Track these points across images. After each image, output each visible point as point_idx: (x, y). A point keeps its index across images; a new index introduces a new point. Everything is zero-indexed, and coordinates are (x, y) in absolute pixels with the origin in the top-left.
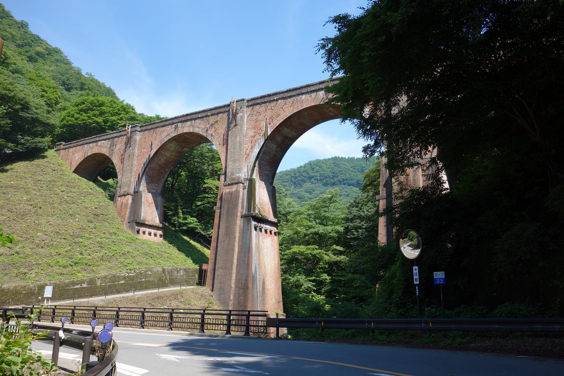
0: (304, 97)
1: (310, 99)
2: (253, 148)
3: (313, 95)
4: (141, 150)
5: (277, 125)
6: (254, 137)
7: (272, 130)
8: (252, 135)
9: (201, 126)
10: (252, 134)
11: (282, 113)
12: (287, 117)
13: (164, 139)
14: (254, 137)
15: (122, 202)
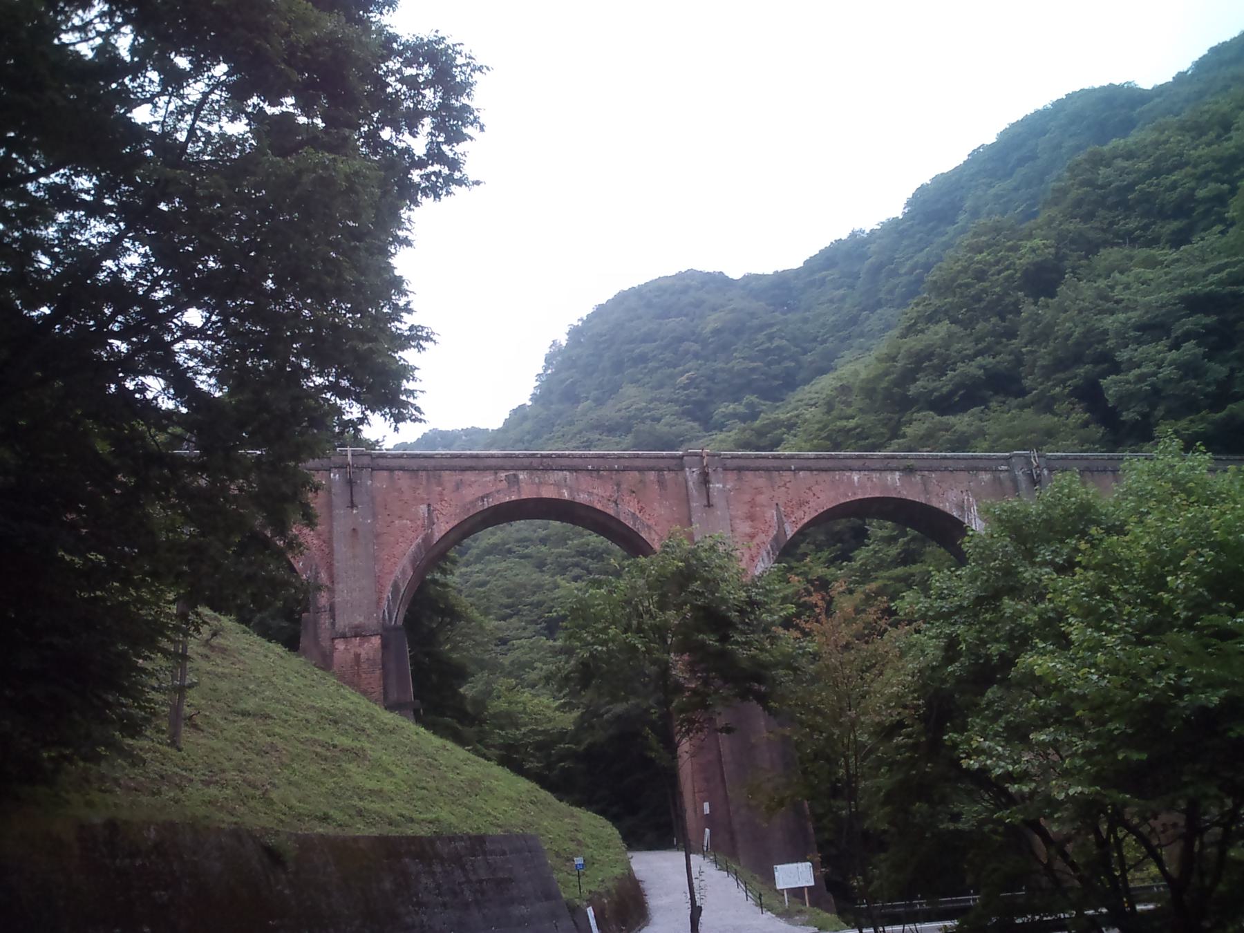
0: (856, 477)
1: (869, 484)
2: (756, 561)
3: (875, 475)
4: (389, 519)
5: (806, 520)
6: (752, 536)
7: (796, 529)
8: (747, 532)
9: (595, 491)
10: (748, 530)
11: (811, 500)
12: (825, 509)
13: (473, 503)
14: (752, 536)
15: (357, 656)
